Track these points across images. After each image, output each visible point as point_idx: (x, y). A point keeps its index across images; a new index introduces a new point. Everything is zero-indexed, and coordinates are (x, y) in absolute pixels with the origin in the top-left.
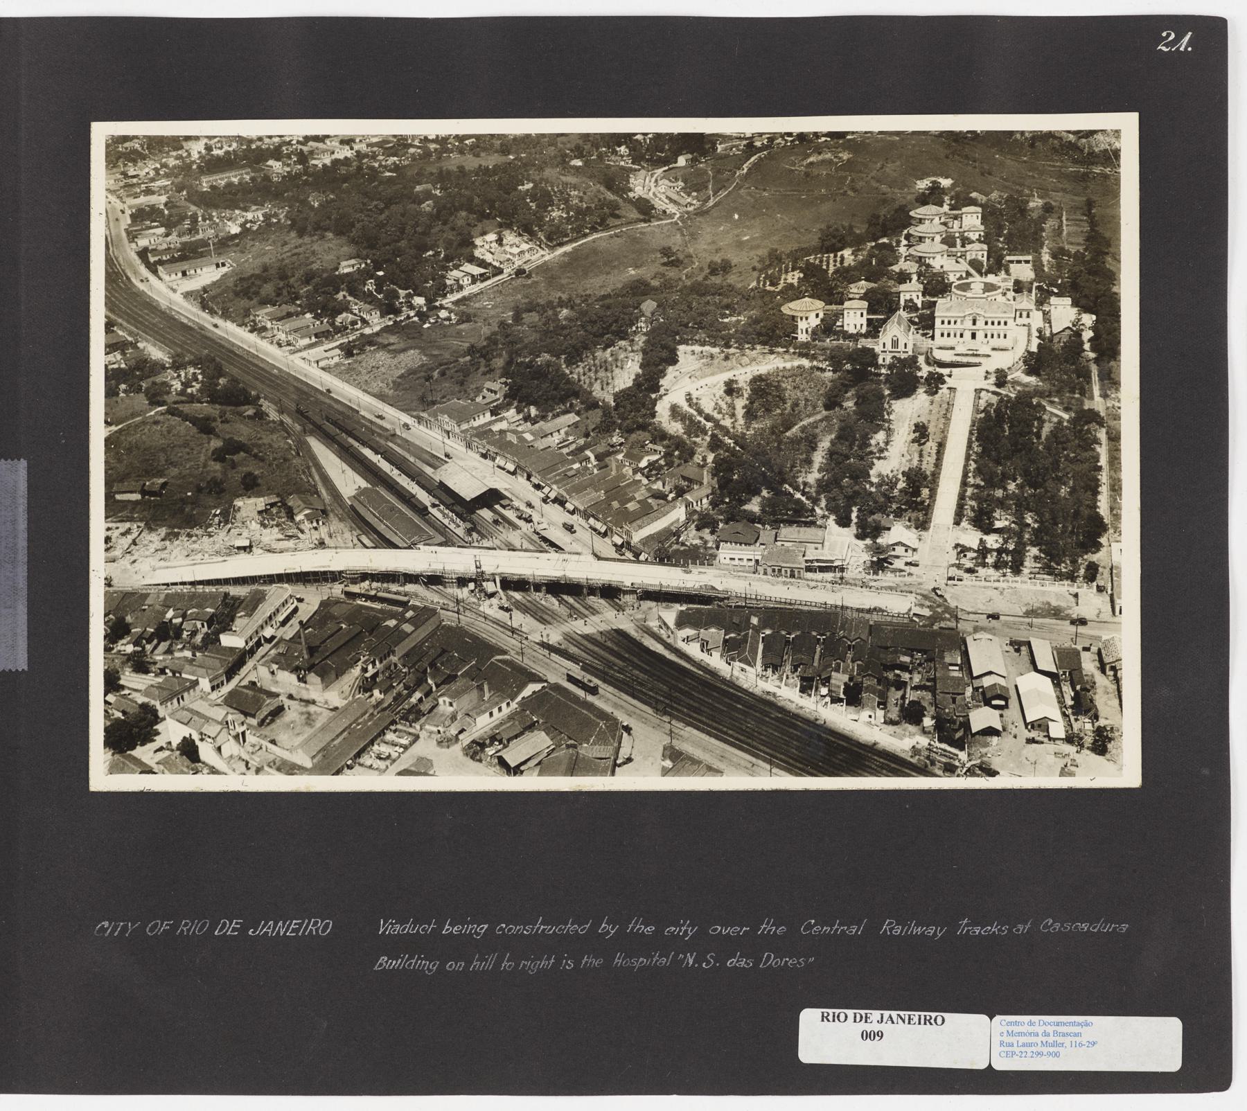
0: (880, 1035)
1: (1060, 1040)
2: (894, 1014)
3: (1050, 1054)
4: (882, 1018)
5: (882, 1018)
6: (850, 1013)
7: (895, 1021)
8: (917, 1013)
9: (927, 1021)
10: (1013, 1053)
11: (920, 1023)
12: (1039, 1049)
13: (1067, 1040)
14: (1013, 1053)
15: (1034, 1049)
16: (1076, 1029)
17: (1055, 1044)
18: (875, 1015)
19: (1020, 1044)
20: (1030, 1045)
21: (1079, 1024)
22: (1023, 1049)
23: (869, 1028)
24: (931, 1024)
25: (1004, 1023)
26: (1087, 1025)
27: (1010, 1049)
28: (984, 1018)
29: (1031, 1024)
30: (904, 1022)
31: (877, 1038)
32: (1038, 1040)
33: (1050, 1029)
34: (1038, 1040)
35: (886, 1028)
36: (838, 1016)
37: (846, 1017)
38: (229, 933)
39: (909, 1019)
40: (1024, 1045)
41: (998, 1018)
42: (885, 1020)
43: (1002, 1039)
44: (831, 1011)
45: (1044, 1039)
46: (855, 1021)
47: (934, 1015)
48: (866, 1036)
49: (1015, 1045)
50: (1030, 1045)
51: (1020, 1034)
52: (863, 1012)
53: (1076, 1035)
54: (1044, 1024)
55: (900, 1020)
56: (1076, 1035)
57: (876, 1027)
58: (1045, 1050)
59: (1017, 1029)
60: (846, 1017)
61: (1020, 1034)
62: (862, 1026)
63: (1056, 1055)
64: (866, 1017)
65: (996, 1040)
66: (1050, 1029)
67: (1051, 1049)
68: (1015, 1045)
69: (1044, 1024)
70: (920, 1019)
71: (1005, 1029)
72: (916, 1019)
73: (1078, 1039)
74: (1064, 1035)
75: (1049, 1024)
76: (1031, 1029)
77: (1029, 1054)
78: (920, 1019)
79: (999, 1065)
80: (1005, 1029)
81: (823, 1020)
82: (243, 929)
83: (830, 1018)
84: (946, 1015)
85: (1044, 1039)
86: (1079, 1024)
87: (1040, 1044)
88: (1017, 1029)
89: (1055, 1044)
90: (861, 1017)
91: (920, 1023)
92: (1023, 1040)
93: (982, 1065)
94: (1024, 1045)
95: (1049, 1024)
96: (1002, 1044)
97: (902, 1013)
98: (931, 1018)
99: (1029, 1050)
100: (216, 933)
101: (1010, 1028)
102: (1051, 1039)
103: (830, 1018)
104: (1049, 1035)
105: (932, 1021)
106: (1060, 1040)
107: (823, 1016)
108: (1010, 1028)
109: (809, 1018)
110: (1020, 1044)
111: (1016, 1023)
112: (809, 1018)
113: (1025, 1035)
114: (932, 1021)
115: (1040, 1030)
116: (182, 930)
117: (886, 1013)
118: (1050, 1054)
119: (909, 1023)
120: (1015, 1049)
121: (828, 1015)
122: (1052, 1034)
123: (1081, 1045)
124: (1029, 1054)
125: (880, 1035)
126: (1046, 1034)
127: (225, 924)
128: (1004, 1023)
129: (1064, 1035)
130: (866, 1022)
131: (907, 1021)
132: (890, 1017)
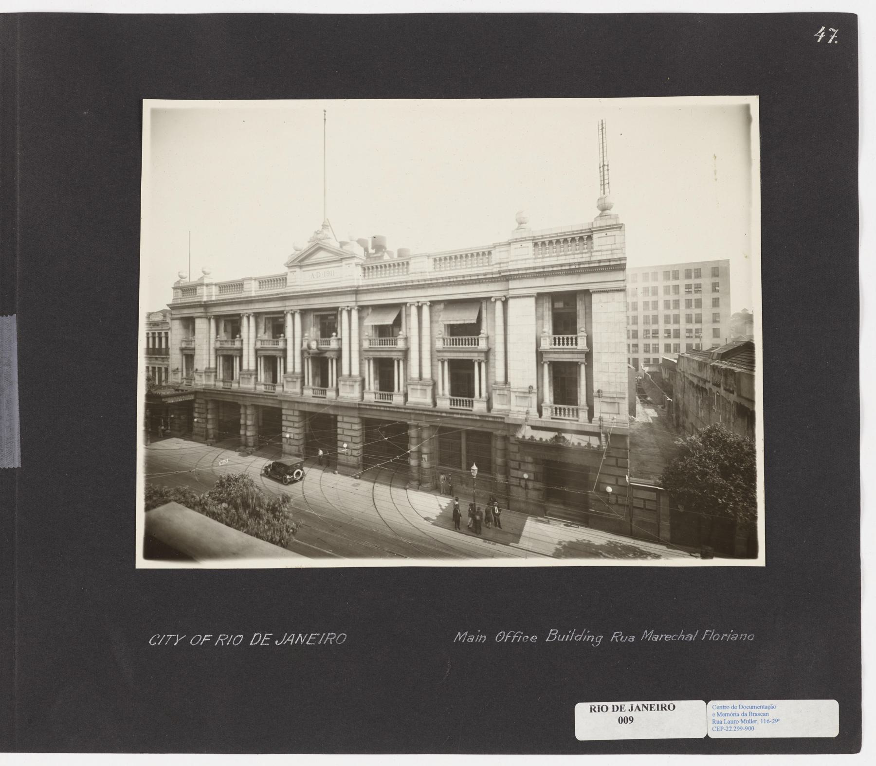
1: (754, 718)
2: (640, 703)
3: (747, 728)
6: (610, 704)
7: (641, 709)
8: (656, 702)
9: (663, 708)
10: (722, 728)
11: (658, 710)
12: (740, 725)
13: (759, 718)
14: (722, 728)
15: (736, 725)
16: (765, 711)
17: (751, 721)
18: (627, 705)
19: (726, 722)
20: (734, 722)
21: (767, 707)
22: (729, 725)
23: (623, 715)
24: (666, 710)
26: (772, 708)
27: (719, 725)
29: (734, 707)
30: (647, 710)
31: (629, 722)
32: (738, 718)
33: (747, 711)
34: (738, 718)
36: (602, 708)
37: (607, 708)
38: (261, 644)
39: (651, 707)
40: (729, 722)
42: (634, 708)
43: (714, 718)
44: (596, 704)
46: (613, 711)
47: (667, 703)
48: (622, 720)
49: (723, 722)
50: (734, 722)
51: (726, 715)
52: (618, 704)
53: (766, 715)
54: (743, 707)
55: (644, 709)
56: (766, 715)
57: (628, 714)
58: (744, 725)
59: (724, 711)
60: (607, 708)
61: (726, 715)
63: (752, 728)
65: (711, 718)
66: (747, 711)
67: (749, 725)
68: (723, 722)
69: (743, 707)
71: (715, 711)
72: (655, 707)
73: (766, 718)
74: (757, 715)
75: (746, 708)
76: (734, 711)
77: (733, 729)
80: (715, 711)
81: (591, 712)
83: (596, 709)
84: (675, 702)
85: (743, 718)
86: (767, 707)
87: (740, 721)
88: (724, 711)
89: (751, 721)
90: (618, 708)
91: (658, 710)
93: (702, 736)
94: (729, 722)
95: (746, 708)
96: (714, 722)
97: (646, 703)
98: (666, 706)
99: (733, 725)
100: (251, 644)
101: (720, 711)
102: (747, 718)
103: (596, 709)
105: (667, 708)
106: (754, 718)
107: (591, 707)
108: (720, 711)
109: (582, 709)
110: (726, 722)
111: (724, 707)
112: (582, 709)
113: (730, 715)
114: (667, 708)
115: (740, 711)
116: (220, 641)
117: (635, 703)
118: (747, 728)
119: (651, 710)
120: (723, 725)
121: (595, 707)
122: (748, 714)
123: (768, 721)
124: (733, 729)
126: (744, 714)
127: (258, 637)
129: (757, 715)
130: (621, 711)
132: (638, 706)
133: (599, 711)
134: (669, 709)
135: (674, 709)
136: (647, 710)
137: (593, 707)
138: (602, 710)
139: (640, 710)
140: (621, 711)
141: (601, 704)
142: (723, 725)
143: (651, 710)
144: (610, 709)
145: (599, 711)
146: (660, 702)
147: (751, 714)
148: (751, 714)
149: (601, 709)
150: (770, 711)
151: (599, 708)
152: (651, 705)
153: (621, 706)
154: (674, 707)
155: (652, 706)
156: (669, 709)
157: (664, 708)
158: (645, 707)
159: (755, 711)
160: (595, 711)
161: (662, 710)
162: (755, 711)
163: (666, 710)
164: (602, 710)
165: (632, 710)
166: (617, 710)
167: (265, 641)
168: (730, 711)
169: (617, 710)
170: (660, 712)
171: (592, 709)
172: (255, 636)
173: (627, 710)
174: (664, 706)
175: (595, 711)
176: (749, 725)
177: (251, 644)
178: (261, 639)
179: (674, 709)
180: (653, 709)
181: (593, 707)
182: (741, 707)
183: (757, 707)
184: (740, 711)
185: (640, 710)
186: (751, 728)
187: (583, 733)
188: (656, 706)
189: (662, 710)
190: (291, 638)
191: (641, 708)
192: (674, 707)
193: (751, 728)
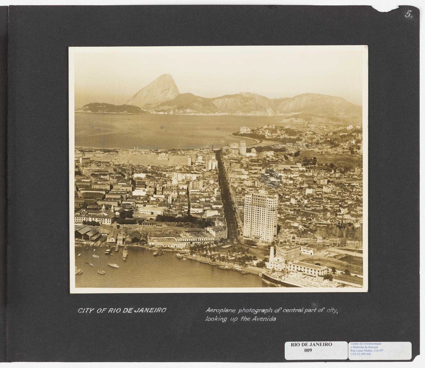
0: (311, 350)
1: (371, 349)
2: (315, 342)
3: (367, 354)
4: (311, 344)
5: (311, 344)
7: (316, 345)
8: (323, 342)
9: (326, 345)
10: (355, 354)
11: (324, 345)
12: (364, 352)
13: (373, 349)
14: (355, 354)
15: (362, 352)
16: (376, 346)
17: (369, 351)
18: (309, 343)
19: (358, 351)
20: (361, 351)
21: (377, 344)
22: (359, 352)
23: (307, 348)
24: (327, 345)
25: (352, 344)
26: (380, 344)
27: (354, 352)
28: (345, 343)
29: (361, 344)
30: (318, 345)
31: (310, 351)
33: (367, 346)
34: (363, 349)
35: (313, 347)
36: (297, 344)
39: (320, 344)
40: (359, 351)
41: (350, 343)
42: (312, 345)
43: (352, 349)
44: (294, 342)
45: (366, 349)
46: (302, 346)
47: (328, 342)
48: (306, 350)
49: (356, 351)
50: (361, 351)
52: (305, 342)
53: (376, 347)
54: (365, 344)
55: (317, 345)
56: (376, 347)
57: (309, 347)
58: (366, 352)
59: (356, 346)
62: (305, 347)
63: (370, 354)
64: (306, 344)
65: (350, 349)
67: (368, 352)
68: (356, 351)
70: (324, 344)
71: (352, 346)
72: (322, 344)
73: (377, 349)
75: (367, 344)
76: (361, 346)
77: (361, 354)
78: (324, 344)
79: (350, 359)
80: (352, 346)
81: (292, 346)
82: (133, 311)
83: (294, 345)
84: (332, 342)
85: (366, 349)
87: (364, 350)
88: (356, 346)
89: (369, 351)
91: (324, 345)
92: (358, 349)
94: (359, 351)
95: (367, 344)
96: (351, 351)
97: (318, 342)
98: (327, 344)
99: (360, 352)
100: (123, 312)
101: (354, 346)
102: (368, 349)
103: (294, 345)
104: (367, 348)
105: (328, 345)
106: (371, 349)
107: (292, 343)
108: (354, 346)
109: (288, 345)
110: (358, 351)
111: (356, 344)
112: (288, 345)
113: (359, 347)
114: (328, 345)
115: (364, 346)
117: (313, 342)
118: (367, 354)
119: (320, 346)
120: (357, 353)
122: (368, 347)
123: (378, 351)
125: (311, 350)
126: (366, 347)
127: (126, 310)
128: (352, 344)
130: (306, 346)
131: (319, 345)
132: (314, 344)
133: (295, 346)
134: (329, 345)
135: (331, 345)
136: (318, 345)
137: (293, 344)
138: (297, 346)
139: (315, 346)
140: (306, 346)
141: (296, 342)
142: (357, 353)
143: (320, 346)
144: (301, 345)
145: (295, 346)
146: (325, 342)
147: (369, 347)
148: (369, 347)
149: (296, 345)
150: (379, 346)
151: (295, 344)
152: (320, 343)
153: (306, 343)
154: (331, 344)
155: (321, 343)
156: (329, 345)
157: (327, 345)
158: (318, 344)
159: (371, 346)
160: (293, 346)
161: (326, 345)
162: (371, 346)
163: (327, 345)
164: (297, 346)
165: (311, 345)
166: (304, 345)
167: (131, 311)
168: (359, 345)
169: (304, 345)
170: (325, 346)
171: (292, 345)
172: (125, 309)
173: (309, 346)
174: (326, 344)
175: (293, 346)
176: (368, 352)
177: (123, 312)
178: (129, 310)
179: (331, 345)
180: (321, 345)
181: (293, 344)
182: (365, 344)
183: (372, 344)
184: (364, 346)
185: (315, 346)
186: (369, 354)
187: (287, 357)
188: (323, 343)
189: (326, 345)
190: (142, 310)
191: (315, 344)
192: (331, 344)
193: (369, 354)
